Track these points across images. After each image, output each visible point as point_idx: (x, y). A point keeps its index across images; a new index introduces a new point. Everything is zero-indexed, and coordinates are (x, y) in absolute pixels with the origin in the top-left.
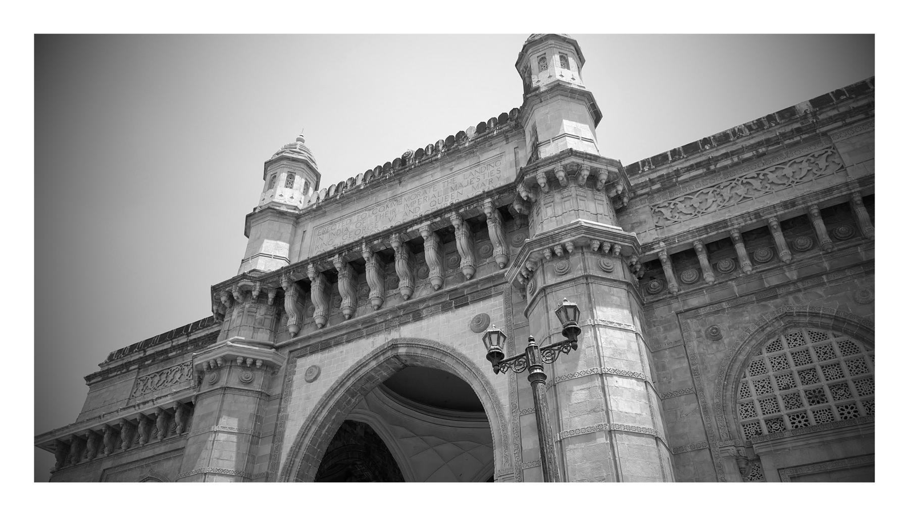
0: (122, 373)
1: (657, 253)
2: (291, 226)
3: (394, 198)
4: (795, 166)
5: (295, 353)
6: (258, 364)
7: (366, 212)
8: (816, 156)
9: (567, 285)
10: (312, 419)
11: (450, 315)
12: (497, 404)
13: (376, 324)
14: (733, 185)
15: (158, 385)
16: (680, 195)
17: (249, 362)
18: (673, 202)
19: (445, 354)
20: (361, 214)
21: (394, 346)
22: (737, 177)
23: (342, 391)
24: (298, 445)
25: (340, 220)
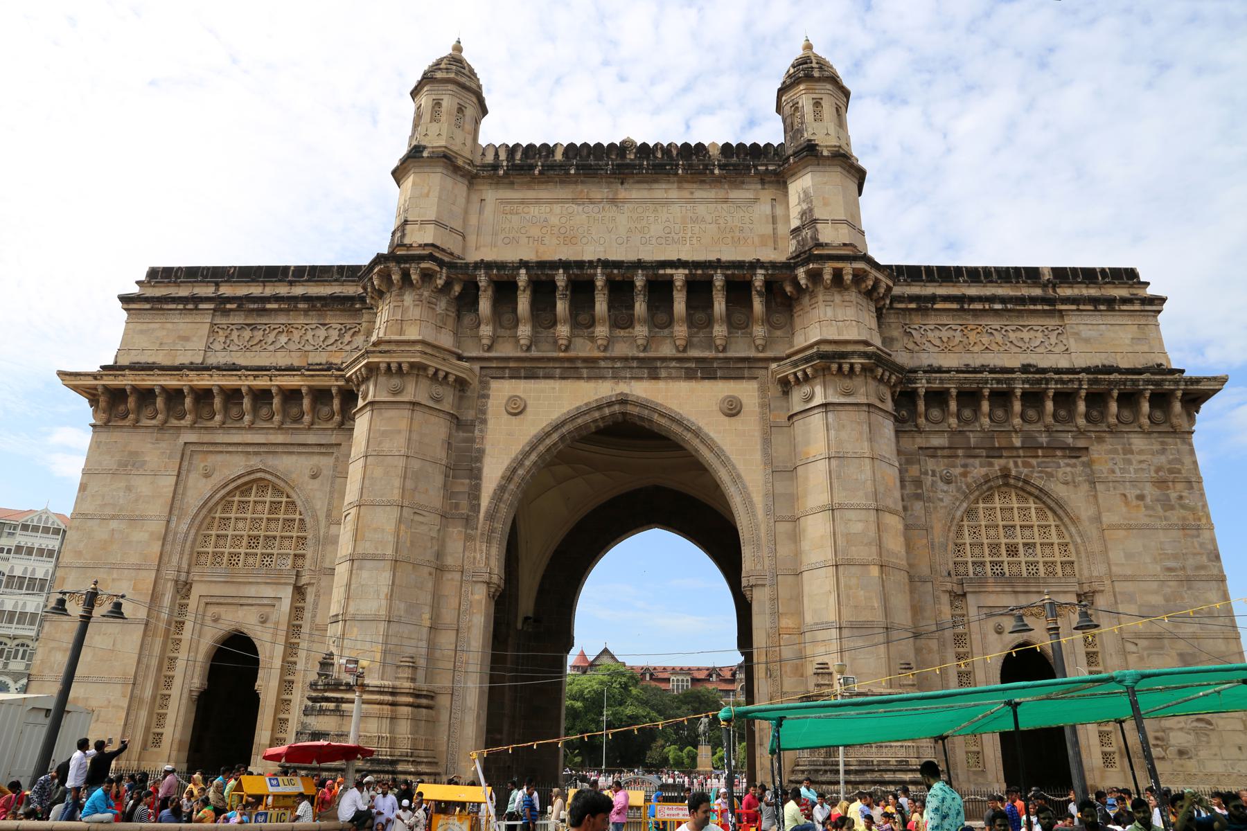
0: (185, 309)
1: (917, 388)
2: (465, 188)
3: (613, 201)
4: (1032, 332)
5: (488, 372)
6: (451, 378)
7: (573, 205)
8: (1050, 329)
9: (850, 408)
11: (693, 384)
12: (748, 500)
13: (599, 368)
14: (979, 330)
15: (251, 343)
16: (932, 321)
17: (441, 375)
18: (924, 327)
19: (688, 429)
20: (567, 205)
21: (623, 401)
22: (983, 323)
23: (555, 437)
24: (501, 489)
25: (536, 203)
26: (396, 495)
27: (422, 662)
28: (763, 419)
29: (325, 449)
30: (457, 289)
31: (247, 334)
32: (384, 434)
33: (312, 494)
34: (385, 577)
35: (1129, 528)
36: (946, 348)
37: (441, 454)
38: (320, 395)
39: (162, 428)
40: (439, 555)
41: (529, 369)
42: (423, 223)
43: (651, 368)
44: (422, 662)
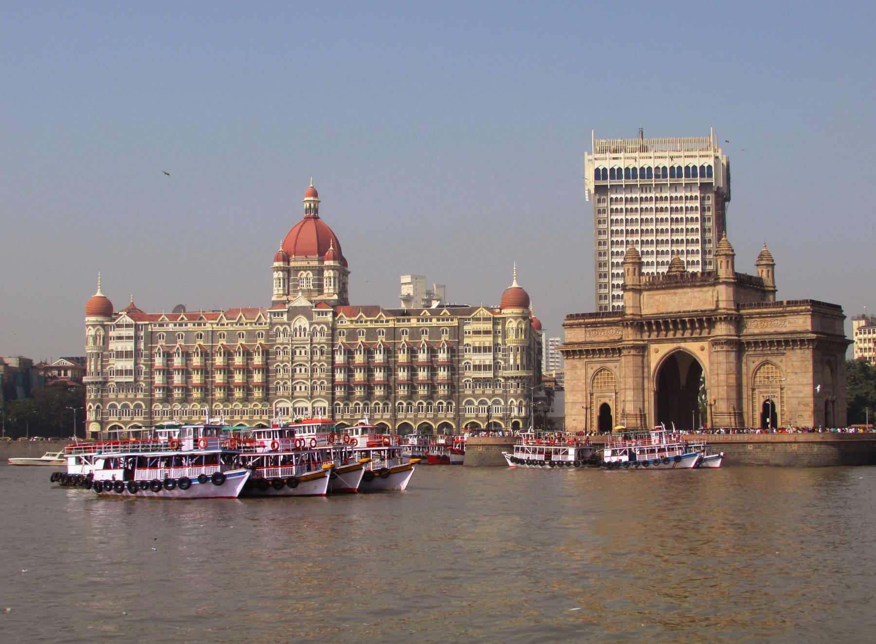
3: (675, 294)
10: (658, 364)
21: (679, 348)
26: (632, 375)
27: (642, 409)
28: (709, 351)
29: (617, 361)
30: (639, 324)
31: (594, 332)
32: (628, 362)
33: (616, 372)
34: (632, 393)
35: (792, 373)
36: (756, 327)
37: (641, 364)
38: (613, 349)
39: (580, 358)
40: (643, 386)
41: (658, 341)
42: (630, 307)
43: (684, 340)
44: (642, 409)
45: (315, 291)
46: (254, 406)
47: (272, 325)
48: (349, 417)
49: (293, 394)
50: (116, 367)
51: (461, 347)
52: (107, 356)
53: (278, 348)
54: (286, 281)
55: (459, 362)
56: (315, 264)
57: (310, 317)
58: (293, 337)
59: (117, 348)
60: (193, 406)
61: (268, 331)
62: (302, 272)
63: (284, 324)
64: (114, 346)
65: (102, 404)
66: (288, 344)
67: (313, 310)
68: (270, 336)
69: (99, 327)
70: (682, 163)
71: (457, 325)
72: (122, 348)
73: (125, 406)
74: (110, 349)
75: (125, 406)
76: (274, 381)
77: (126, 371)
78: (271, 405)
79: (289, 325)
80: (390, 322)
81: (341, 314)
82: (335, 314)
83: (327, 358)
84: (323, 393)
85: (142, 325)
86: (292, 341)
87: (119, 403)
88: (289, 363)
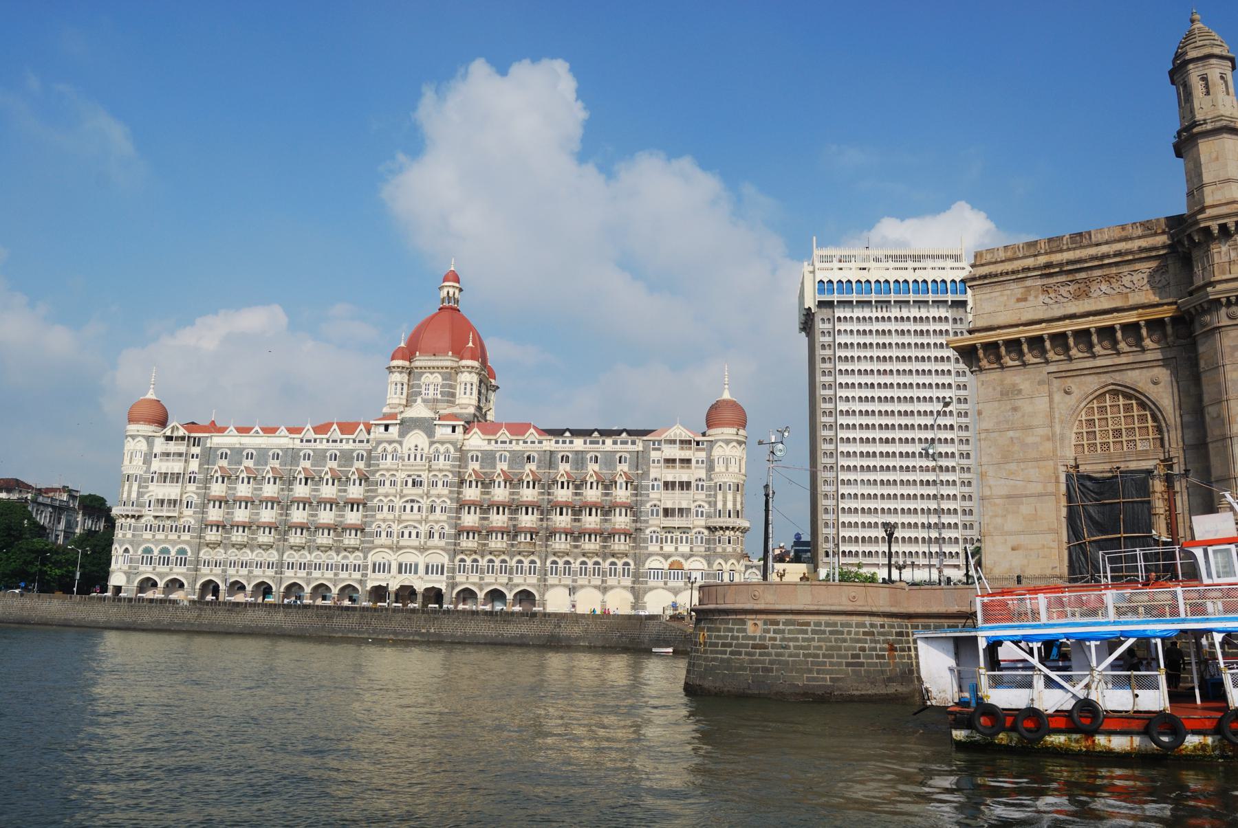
45: (442, 401)
46: (345, 557)
47: (379, 443)
48: (477, 580)
49: (398, 542)
50: (157, 494)
51: (644, 483)
52: (146, 480)
53: (383, 475)
54: (405, 387)
55: (643, 503)
56: (449, 364)
57: (430, 432)
58: (404, 460)
59: (160, 468)
60: (257, 555)
61: (369, 452)
62: (428, 375)
63: (394, 442)
64: (158, 465)
65: (133, 547)
66: (397, 471)
67: (435, 422)
68: (369, 458)
69: (140, 438)
70: (929, 276)
71: (641, 449)
72: (167, 468)
73: (165, 551)
74: (152, 470)
75: (165, 551)
76: (373, 522)
77: (169, 501)
78: (365, 558)
79: (400, 443)
80: (544, 442)
81: (476, 429)
82: (466, 431)
83: (451, 492)
84: (442, 543)
85: (199, 439)
86: (403, 465)
87: (157, 542)
88: (396, 497)
